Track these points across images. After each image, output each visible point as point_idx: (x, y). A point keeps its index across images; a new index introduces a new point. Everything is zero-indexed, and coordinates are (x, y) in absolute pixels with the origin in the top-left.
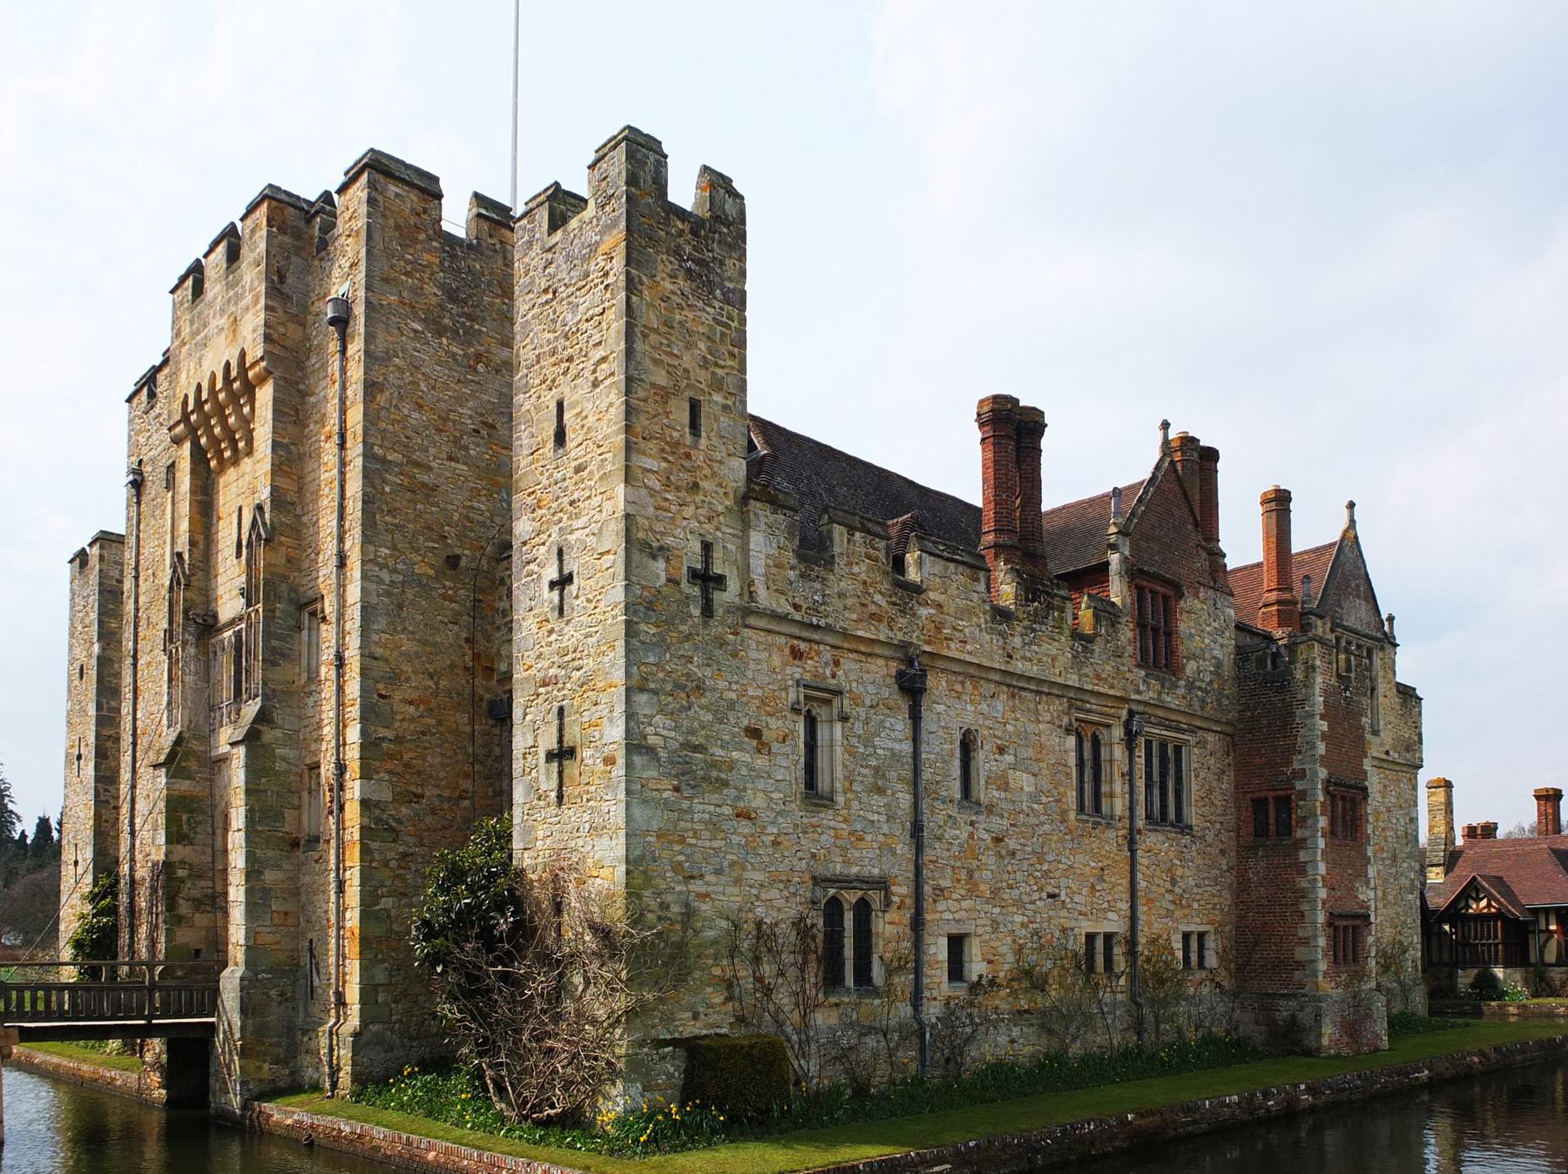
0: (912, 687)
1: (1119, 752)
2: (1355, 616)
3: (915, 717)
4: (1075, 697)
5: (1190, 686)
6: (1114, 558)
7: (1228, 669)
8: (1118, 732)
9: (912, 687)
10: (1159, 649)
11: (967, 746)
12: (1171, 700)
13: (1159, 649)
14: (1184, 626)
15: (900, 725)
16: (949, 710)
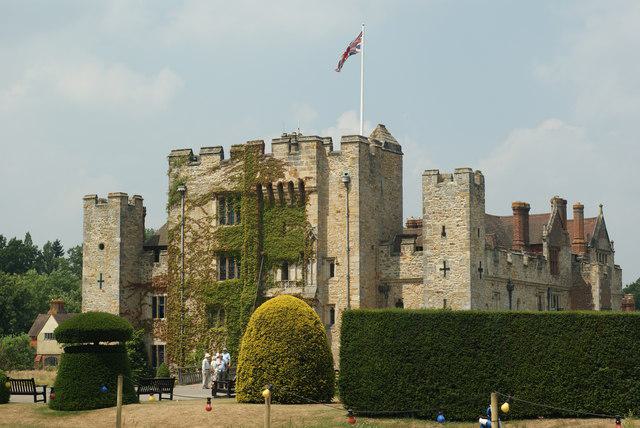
0: (510, 290)
1: (546, 301)
2: (602, 245)
3: (510, 297)
4: (537, 286)
5: (562, 278)
6: (545, 244)
7: (570, 271)
8: (546, 294)
9: (510, 290)
10: (554, 271)
11: (518, 301)
12: (557, 283)
13: (554, 271)
14: (560, 260)
15: (507, 299)
16: (516, 294)
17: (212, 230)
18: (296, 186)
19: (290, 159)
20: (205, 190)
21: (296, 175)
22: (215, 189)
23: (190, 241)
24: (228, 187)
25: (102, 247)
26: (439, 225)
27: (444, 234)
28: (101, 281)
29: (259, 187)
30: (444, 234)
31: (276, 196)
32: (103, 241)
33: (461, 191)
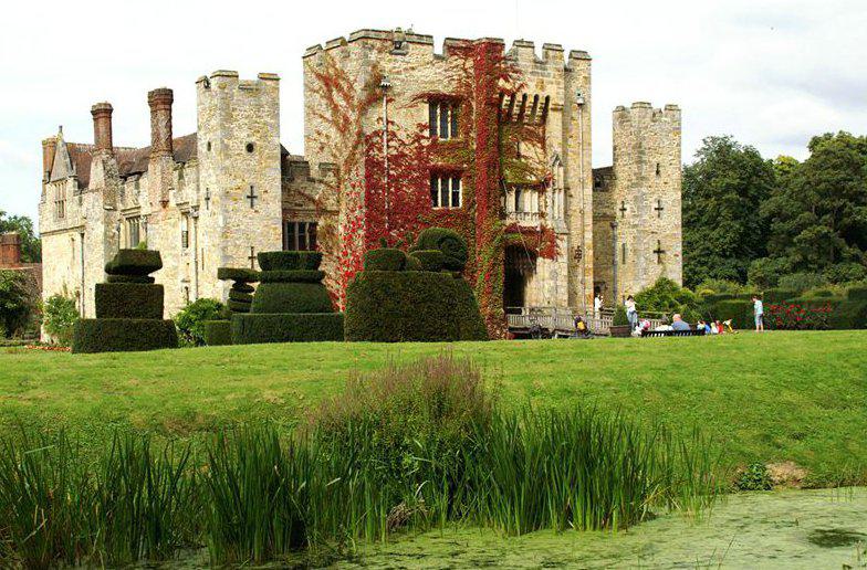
17: (425, 143)
18: (542, 100)
19: (537, 67)
20: (415, 89)
21: (542, 88)
22: (428, 89)
23: (395, 153)
24: (446, 88)
25: (250, 148)
26: (654, 161)
27: (658, 172)
28: (252, 197)
29: (502, 96)
30: (658, 172)
31: (516, 110)
32: (253, 139)
33: (674, 129)
